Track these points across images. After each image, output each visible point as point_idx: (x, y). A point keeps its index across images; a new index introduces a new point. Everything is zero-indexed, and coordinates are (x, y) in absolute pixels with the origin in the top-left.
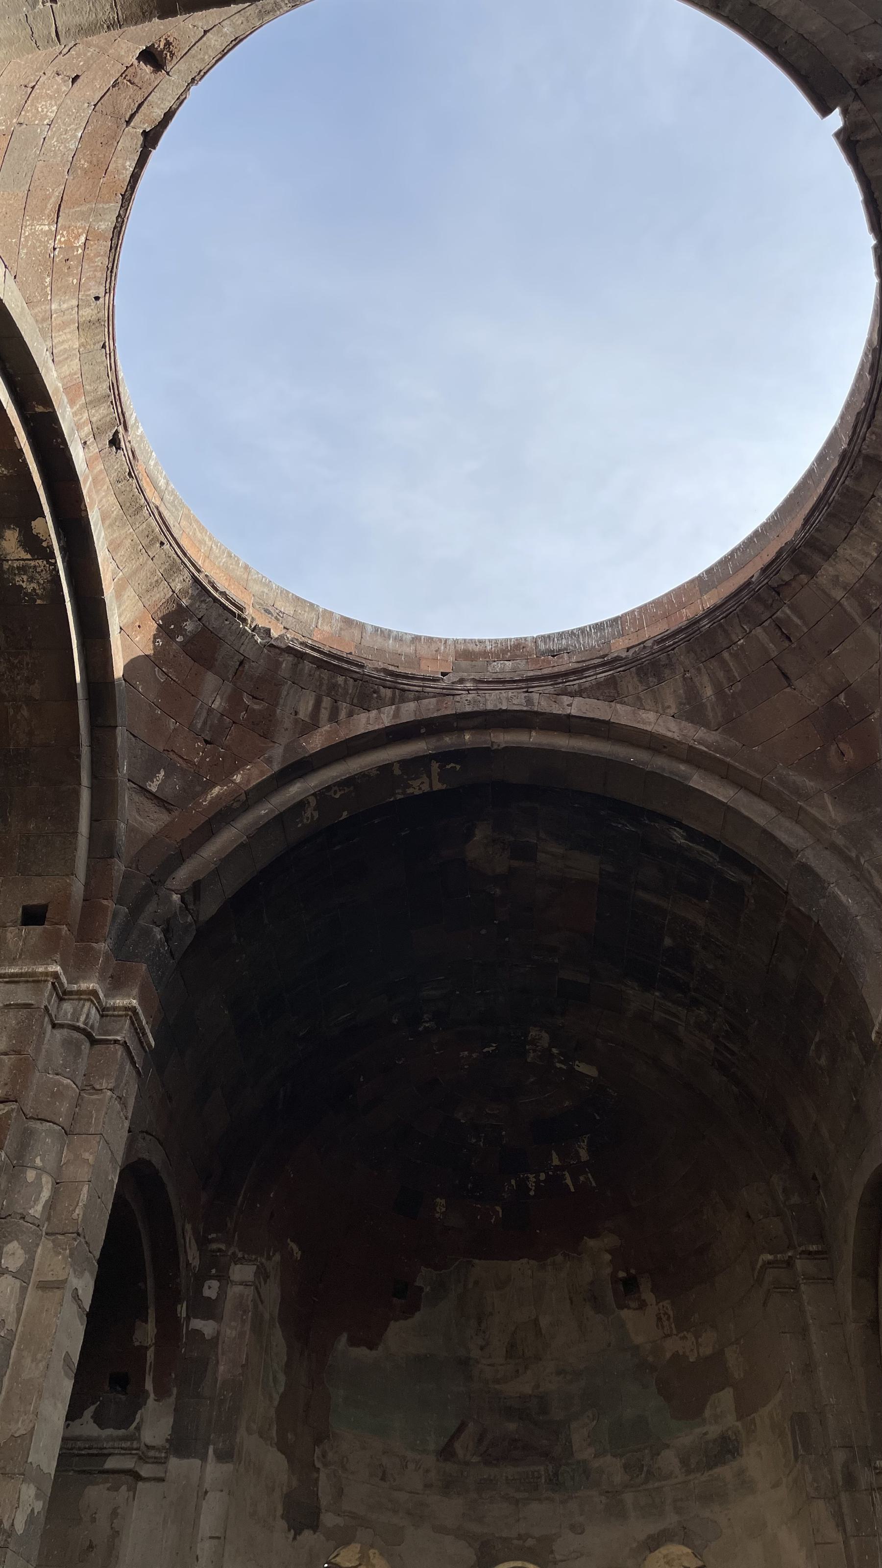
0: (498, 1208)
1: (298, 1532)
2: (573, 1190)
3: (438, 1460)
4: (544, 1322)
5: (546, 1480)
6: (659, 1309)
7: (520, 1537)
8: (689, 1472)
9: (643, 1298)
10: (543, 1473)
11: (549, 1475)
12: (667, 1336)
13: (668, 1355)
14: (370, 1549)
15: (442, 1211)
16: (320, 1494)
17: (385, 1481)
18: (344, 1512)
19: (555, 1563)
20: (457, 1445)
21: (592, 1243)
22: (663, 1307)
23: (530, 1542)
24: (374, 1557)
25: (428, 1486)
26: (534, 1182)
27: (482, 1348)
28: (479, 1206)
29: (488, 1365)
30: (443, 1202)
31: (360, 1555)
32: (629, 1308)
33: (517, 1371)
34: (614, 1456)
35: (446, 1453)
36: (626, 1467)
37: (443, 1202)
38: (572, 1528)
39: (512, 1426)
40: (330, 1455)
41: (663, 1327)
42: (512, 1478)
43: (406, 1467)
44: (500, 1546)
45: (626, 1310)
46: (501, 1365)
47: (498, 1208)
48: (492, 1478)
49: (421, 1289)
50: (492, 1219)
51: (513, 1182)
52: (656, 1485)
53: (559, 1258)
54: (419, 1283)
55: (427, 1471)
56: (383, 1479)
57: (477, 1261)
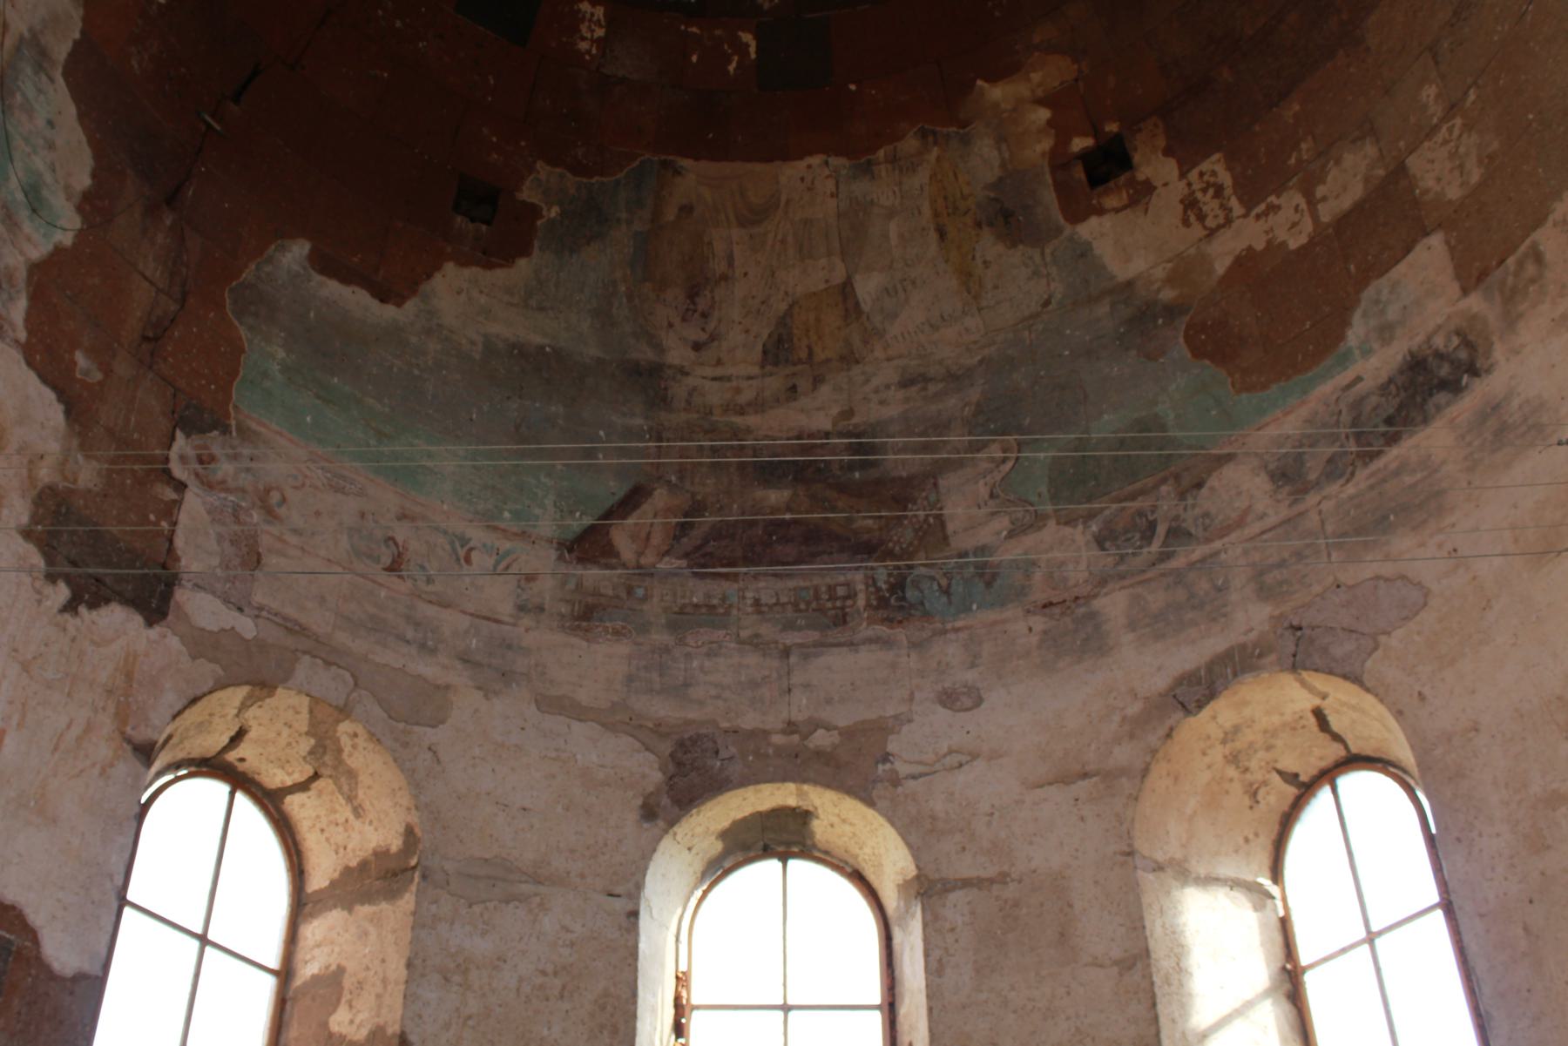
0: (747, 37)
1: (86, 595)
3: (560, 558)
4: (867, 288)
5: (868, 600)
7: (791, 727)
10: (860, 587)
11: (879, 590)
14: (338, 721)
15: (596, 36)
16: (179, 542)
17: (400, 577)
18: (261, 608)
19: (895, 781)
20: (622, 537)
21: (997, 93)
23: (821, 739)
24: (354, 747)
27: (697, 347)
28: (694, 30)
29: (714, 379)
30: (599, 12)
31: (313, 741)
32: (1100, 211)
33: (794, 388)
34: (1067, 523)
36: (1100, 542)
37: (599, 12)
38: (948, 699)
39: (776, 496)
40: (225, 469)
42: (774, 601)
43: (468, 560)
44: (733, 750)
45: (1094, 221)
46: (750, 378)
47: (747, 37)
48: (715, 602)
49: (533, 211)
50: (730, 62)
53: (910, 144)
54: (527, 194)
56: (394, 567)
57: (686, 163)
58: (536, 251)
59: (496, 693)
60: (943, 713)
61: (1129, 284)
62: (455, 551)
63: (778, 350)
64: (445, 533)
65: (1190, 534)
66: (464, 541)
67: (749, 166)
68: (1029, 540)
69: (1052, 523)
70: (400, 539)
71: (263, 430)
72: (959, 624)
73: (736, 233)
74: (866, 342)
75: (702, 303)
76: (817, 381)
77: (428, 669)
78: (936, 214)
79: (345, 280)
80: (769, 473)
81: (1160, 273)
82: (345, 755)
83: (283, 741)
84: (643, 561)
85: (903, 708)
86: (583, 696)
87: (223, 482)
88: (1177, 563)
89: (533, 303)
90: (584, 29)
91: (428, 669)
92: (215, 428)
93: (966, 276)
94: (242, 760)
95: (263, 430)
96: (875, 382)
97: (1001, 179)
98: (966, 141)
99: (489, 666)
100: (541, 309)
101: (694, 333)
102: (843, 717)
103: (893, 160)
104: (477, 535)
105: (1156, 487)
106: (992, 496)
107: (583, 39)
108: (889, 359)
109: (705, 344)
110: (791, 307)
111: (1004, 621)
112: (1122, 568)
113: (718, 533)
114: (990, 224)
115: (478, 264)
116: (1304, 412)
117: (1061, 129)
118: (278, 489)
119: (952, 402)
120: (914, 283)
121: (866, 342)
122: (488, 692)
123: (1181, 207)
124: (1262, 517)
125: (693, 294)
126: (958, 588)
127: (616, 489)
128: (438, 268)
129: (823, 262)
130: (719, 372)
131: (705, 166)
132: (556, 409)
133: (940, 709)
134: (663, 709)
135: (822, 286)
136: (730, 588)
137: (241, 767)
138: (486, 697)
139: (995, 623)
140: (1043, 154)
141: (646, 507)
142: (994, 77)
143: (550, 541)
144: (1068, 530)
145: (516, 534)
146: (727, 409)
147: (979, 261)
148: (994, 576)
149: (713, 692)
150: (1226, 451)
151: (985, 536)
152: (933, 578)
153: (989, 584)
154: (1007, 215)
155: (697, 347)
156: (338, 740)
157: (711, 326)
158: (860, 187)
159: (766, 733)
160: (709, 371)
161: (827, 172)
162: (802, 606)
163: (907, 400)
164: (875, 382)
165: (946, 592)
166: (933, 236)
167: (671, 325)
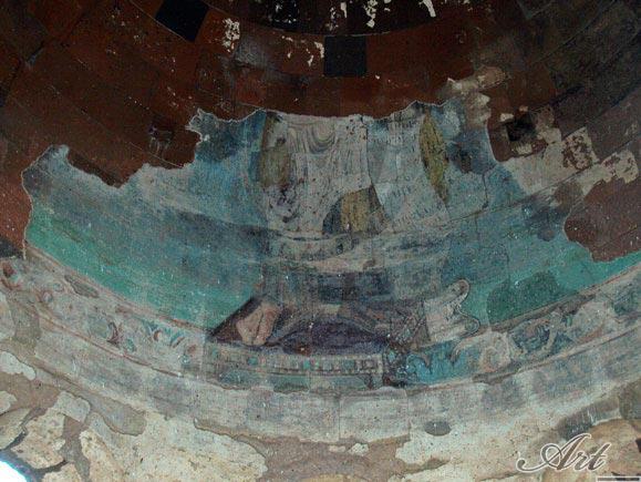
0: (319, 45)
2: (433, 14)
3: (207, 339)
4: (383, 192)
6: (567, 143)
8: (631, 320)
9: (539, 138)
10: (380, 362)
12: (580, 171)
13: (586, 191)
17: (117, 347)
20: (243, 327)
21: (458, 86)
22: (574, 138)
23: (358, 449)
25: (187, 368)
26: (375, 7)
27: (286, 220)
30: (237, 25)
31: (64, 442)
32: (516, 155)
33: (341, 247)
35: (222, 332)
37: (237, 25)
39: (332, 309)
40: (19, 279)
41: (575, 162)
43: (156, 338)
45: (512, 160)
46: (316, 239)
47: (319, 45)
49: (195, 137)
51: (343, 7)
52: (572, 352)
53: (409, 112)
54: (191, 127)
55: (192, 349)
56: (114, 342)
57: (282, 114)
58: (195, 161)
59: (171, 417)
60: (427, 437)
61: (533, 198)
62: (148, 331)
63: (332, 223)
64: (143, 321)
65: (568, 340)
66: (154, 327)
67: (317, 118)
68: (476, 339)
69: (489, 330)
70: (117, 324)
71: (41, 256)
72: (437, 385)
73: (309, 156)
74: (382, 221)
75: (289, 195)
76: (355, 243)
77: (133, 401)
78: (423, 152)
79: (88, 171)
80: (326, 294)
81: (550, 192)
82: (83, 450)
83: (47, 441)
84: (255, 343)
85: (404, 433)
86: (222, 420)
87: (18, 286)
88: (562, 355)
89: (193, 189)
90: (227, 34)
91: (133, 401)
92: (13, 254)
93: (439, 188)
94: (21, 451)
95: (41, 256)
96: (388, 244)
97: (460, 134)
98: (441, 111)
99: (168, 401)
100: (198, 194)
101: (284, 212)
102: (372, 437)
103: (399, 120)
104: (162, 323)
105: (549, 312)
106: (454, 313)
107: (228, 40)
108: (395, 233)
109: (291, 218)
110: (340, 200)
111: (462, 385)
112: (530, 357)
113: (301, 328)
114: (454, 160)
115: (163, 165)
116: (634, 274)
117: (495, 109)
118: (49, 291)
119: (431, 260)
120: (409, 190)
121: (382, 221)
122: (167, 416)
123: (562, 157)
124: (610, 331)
125: (283, 192)
126: (435, 366)
127: (238, 300)
128: (140, 167)
129: (359, 175)
130: (298, 235)
131: (292, 116)
132: (206, 252)
133: (427, 435)
134: (269, 430)
135: (358, 189)
136: (305, 360)
137: (20, 456)
138: (166, 419)
139: (456, 386)
140: (484, 122)
141: (258, 311)
142: (457, 78)
143: (203, 328)
144: (498, 334)
145: (182, 324)
146: (304, 256)
147: (447, 179)
148: (457, 358)
149: (296, 420)
150: (590, 293)
151: (451, 336)
152: (421, 359)
153: (453, 363)
154: (464, 155)
155: (286, 220)
156: (79, 441)
157: (293, 209)
158: (381, 134)
159: (327, 445)
160: (292, 235)
161: (361, 125)
162: (347, 372)
163: (406, 256)
164: (388, 244)
165: (430, 368)
166: (421, 163)
167: (271, 207)
